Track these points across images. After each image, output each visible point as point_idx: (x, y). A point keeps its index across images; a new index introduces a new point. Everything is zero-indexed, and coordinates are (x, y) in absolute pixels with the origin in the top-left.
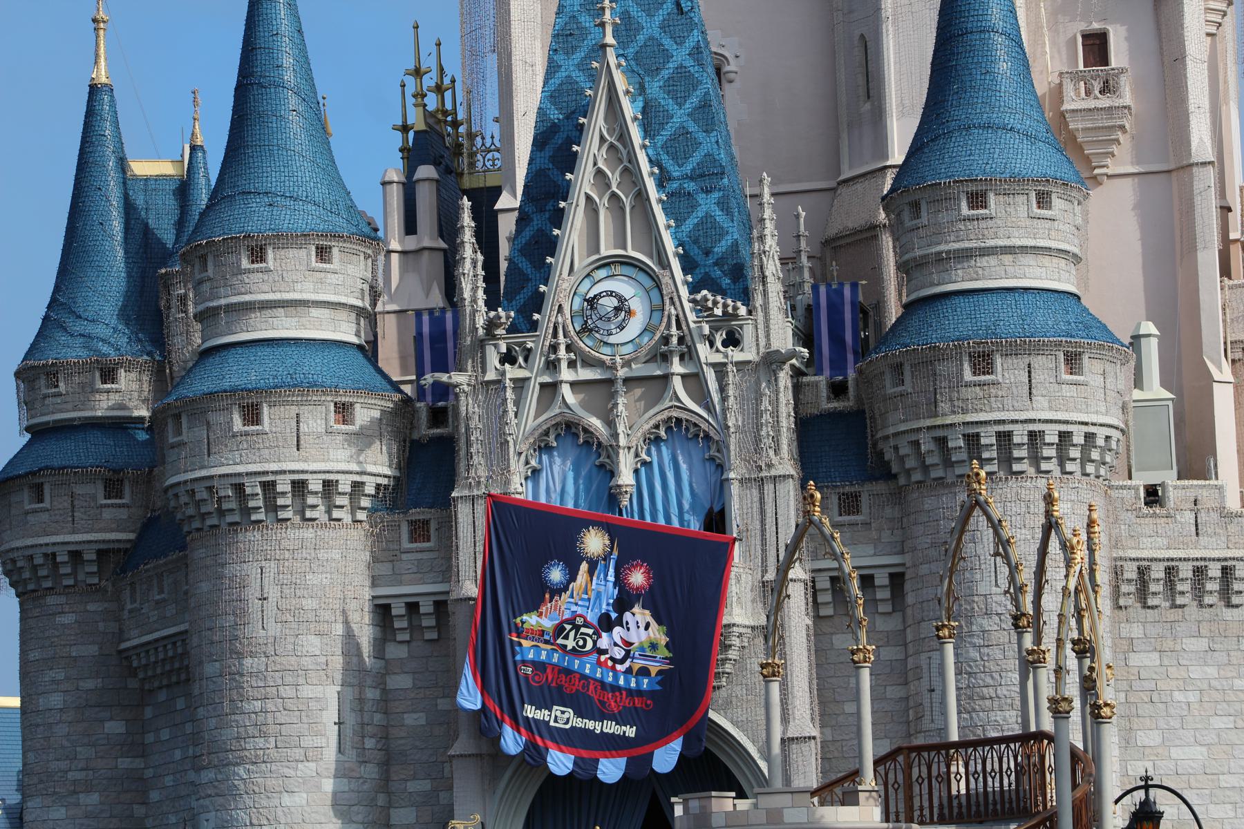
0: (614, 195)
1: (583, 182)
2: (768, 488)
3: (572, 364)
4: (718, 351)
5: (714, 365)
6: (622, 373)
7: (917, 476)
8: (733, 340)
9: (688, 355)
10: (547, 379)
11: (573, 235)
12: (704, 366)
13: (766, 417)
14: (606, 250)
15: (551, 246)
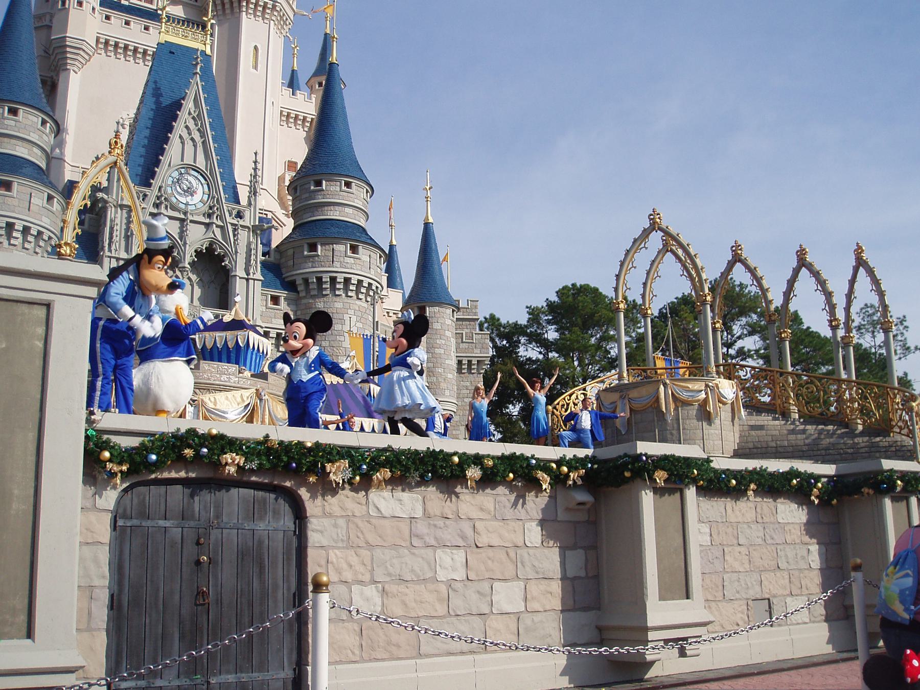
0: (192, 139)
1: (179, 128)
2: (251, 282)
3: (166, 208)
4: (233, 219)
5: (232, 224)
6: (190, 218)
7: (314, 293)
8: (239, 215)
9: (221, 217)
10: (155, 211)
11: (173, 151)
12: (228, 224)
13: (253, 252)
14: (188, 160)
15: (162, 151)
